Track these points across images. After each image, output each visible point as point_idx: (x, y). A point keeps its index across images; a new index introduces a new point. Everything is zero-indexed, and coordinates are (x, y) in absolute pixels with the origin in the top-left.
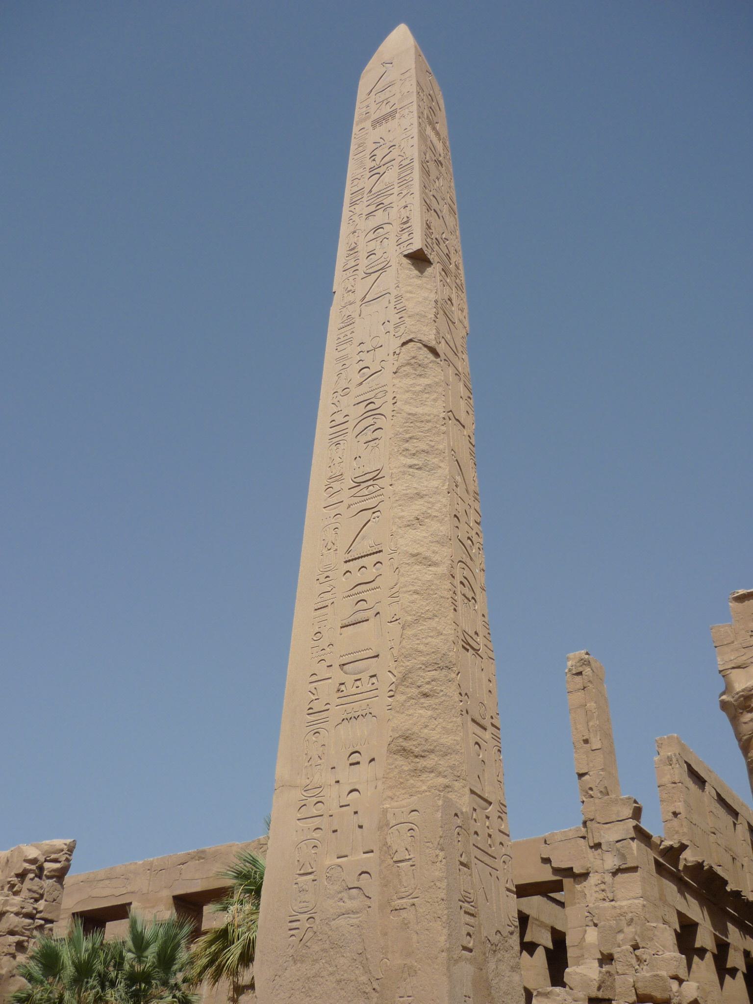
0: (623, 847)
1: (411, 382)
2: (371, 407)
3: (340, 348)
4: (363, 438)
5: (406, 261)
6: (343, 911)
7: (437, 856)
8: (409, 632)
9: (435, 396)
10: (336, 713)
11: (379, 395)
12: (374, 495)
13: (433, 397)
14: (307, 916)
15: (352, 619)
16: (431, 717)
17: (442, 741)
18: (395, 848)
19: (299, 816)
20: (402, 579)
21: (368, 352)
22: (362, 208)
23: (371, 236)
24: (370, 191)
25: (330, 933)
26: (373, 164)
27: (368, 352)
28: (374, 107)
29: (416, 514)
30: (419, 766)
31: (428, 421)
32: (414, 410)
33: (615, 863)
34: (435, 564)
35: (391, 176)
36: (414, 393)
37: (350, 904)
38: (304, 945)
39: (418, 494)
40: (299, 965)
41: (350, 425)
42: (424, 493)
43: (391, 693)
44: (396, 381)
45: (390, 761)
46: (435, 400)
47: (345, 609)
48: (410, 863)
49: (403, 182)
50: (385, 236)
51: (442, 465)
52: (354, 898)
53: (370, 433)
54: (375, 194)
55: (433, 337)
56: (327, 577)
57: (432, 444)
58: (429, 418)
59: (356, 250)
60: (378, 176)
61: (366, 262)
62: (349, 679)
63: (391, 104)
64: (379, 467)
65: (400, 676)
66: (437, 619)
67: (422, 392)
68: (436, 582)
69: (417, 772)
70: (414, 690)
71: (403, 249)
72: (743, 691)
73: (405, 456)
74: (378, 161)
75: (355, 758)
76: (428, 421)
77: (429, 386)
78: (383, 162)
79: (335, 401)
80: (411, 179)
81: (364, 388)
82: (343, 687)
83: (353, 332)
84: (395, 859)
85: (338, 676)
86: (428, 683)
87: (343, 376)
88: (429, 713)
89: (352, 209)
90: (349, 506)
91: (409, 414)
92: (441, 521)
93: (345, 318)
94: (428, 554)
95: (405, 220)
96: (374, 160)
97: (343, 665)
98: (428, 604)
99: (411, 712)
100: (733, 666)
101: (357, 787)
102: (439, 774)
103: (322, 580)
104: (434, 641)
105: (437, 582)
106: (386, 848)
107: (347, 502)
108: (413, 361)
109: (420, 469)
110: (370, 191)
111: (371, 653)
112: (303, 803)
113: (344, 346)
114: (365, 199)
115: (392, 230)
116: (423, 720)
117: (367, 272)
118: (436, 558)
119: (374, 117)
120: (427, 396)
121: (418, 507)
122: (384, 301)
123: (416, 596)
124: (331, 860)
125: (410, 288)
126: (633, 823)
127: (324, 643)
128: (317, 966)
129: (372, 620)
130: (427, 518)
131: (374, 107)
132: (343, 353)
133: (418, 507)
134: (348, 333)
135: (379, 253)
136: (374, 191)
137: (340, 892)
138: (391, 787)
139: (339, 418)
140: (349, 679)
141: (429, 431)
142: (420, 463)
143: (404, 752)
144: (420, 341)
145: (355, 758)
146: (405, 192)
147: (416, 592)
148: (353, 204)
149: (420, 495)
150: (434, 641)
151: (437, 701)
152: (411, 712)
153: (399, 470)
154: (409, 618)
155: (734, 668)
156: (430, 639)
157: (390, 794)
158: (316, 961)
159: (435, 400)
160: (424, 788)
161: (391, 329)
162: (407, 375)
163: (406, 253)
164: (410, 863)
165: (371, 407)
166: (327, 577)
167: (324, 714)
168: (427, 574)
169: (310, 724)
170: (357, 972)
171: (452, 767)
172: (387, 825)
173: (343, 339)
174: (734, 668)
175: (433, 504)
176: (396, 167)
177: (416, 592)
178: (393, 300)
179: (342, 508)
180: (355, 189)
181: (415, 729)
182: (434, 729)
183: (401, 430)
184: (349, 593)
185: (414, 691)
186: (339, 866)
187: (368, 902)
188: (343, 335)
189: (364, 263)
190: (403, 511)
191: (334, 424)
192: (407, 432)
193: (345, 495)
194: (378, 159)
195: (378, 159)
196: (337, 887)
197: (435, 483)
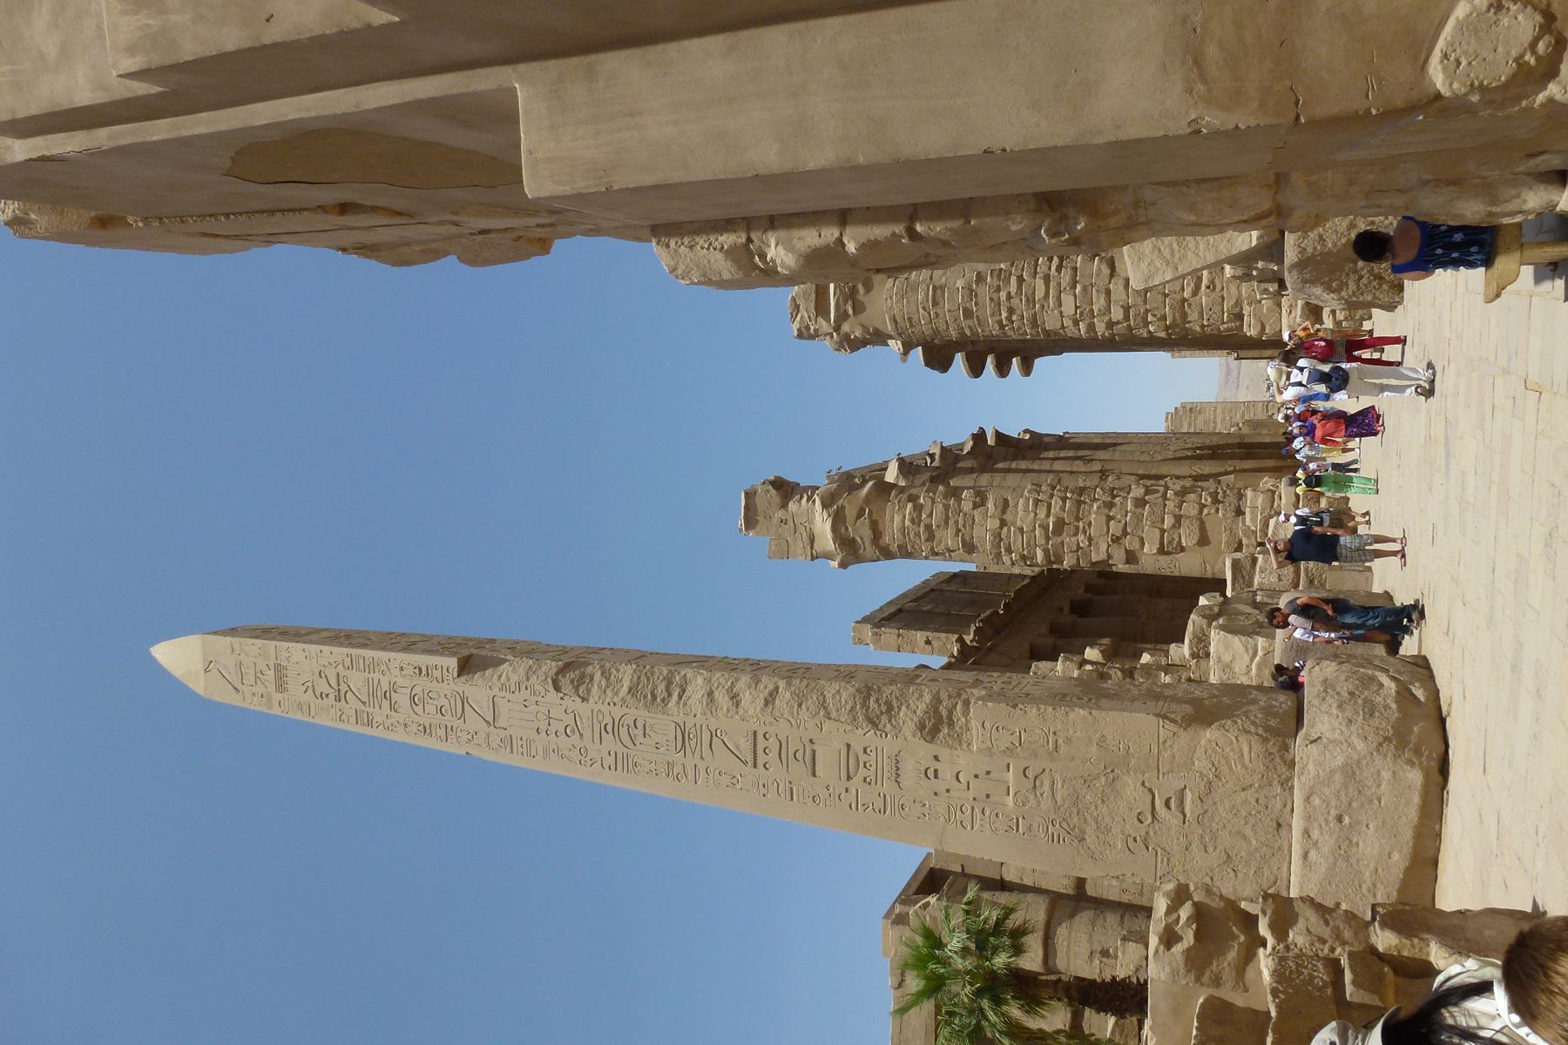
1: (596, 686)
2: (609, 728)
3: (533, 753)
4: (640, 738)
5: (463, 678)
6: (1050, 793)
7: (1021, 709)
8: (834, 715)
9: (613, 670)
10: (888, 787)
11: (600, 717)
12: (699, 733)
13: (615, 672)
15: (809, 763)
16: (908, 707)
17: (928, 701)
18: (1009, 745)
19: (969, 828)
20: (786, 715)
22: (379, 715)
23: (419, 709)
24: (364, 703)
25: (1066, 806)
26: (332, 697)
28: (259, 689)
29: (727, 698)
30: (945, 721)
31: (639, 678)
32: (625, 689)
34: (777, 689)
35: (356, 680)
36: (607, 687)
37: (1046, 788)
38: (1072, 830)
39: (709, 695)
40: (1086, 837)
41: (620, 749)
42: (708, 689)
43: (883, 735)
44: (591, 700)
45: (939, 742)
46: (618, 671)
47: (799, 770)
48: (1022, 732)
49: (372, 667)
50: (426, 692)
51: (683, 673)
52: (1042, 783)
53: (636, 731)
55: (554, 664)
56: (764, 787)
57: (661, 678)
58: (635, 678)
59: (428, 727)
60: (349, 693)
61: (448, 717)
62: (862, 772)
63: (265, 668)
64: (673, 725)
65: (870, 726)
66: (826, 693)
67: (608, 679)
68: (793, 689)
69: (951, 724)
70: (883, 718)
71: (450, 678)
72: (835, 543)
73: (669, 701)
74: (331, 691)
75: (931, 774)
76: (639, 678)
77: (603, 673)
78: (335, 687)
79: (589, 763)
80: (371, 659)
81: (587, 734)
82: (868, 780)
83: (521, 739)
84: (1017, 745)
85: (857, 780)
86: (879, 706)
87: (566, 752)
88: (904, 708)
89: (375, 725)
90: (702, 758)
91: (629, 692)
92: (737, 680)
93: (502, 745)
94: (767, 692)
95: (417, 671)
96: (327, 695)
98: (812, 698)
99: (901, 722)
100: (809, 547)
101: (954, 774)
102: (955, 707)
104: (844, 696)
105: (793, 689)
106: (1009, 751)
107: (697, 760)
108: (576, 683)
109: (684, 691)
110: (364, 703)
113: (533, 749)
114: (371, 710)
115: (422, 684)
116: (909, 713)
117: (459, 716)
118: (771, 687)
119: (272, 688)
120: (612, 677)
121: (721, 697)
122: (500, 702)
123: (803, 706)
124: (1010, 800)
125: (495, 677)
127: (823, 793)
128: (1089, 819)
129: (815, 747)
130: (732, 690)
131: (259, 689)
132: (540, 752)
133: (721, 697)
134: (520, 743)
135: (443, 701)
136: (365, 699)
137: (1036, 795)
138: (960, 744)
139: (610, 761)
141: (648, 680)
142: (678, 690)
143: (935, 730)
144: (557, 674)
145: (931, 774)
146: (384, 667)
147: (800, 705)
148: (370, 724)
149: (710, 694)
150: (844, 696)
151: (894, 701)
152: (901, 722)
153: (681, 707)
154: (822, 713)
155: (812, 548)
156: (843, 700)
157: (965, 745)
158: (1085, 820)
159: (618, 671)
160: (963, 719)
161: (534, 699)
162: (589, 691)
163: (456, 674)
164: (1022, 732)
165: (609, 728)
166: (764, 787)
167: (888, 797)
168: (785, 695)
170: (1097, 785)
171: (950, 697)
172: (990, 749)
173: (525, 750)
174: (812, 548)
175: (719, 684)
176: (348, 673)
177: (800, 705)
178: (503, 694)
179: (701, 766)
180: (353, 719)
181: (916, 719)
182: (918, 707)
183: (643, 701)
184: (785, 766)
185: (884, 718)
186: (1016, 794)
187: (1047, 771)
189: (448, 720)
190: (722, 708)
191: (613, 768)
192: (645, 697)
193: (690, 762)
194: (327, 690)
195: (327, 690)
196: (1032, 797)
197: (700, 680)
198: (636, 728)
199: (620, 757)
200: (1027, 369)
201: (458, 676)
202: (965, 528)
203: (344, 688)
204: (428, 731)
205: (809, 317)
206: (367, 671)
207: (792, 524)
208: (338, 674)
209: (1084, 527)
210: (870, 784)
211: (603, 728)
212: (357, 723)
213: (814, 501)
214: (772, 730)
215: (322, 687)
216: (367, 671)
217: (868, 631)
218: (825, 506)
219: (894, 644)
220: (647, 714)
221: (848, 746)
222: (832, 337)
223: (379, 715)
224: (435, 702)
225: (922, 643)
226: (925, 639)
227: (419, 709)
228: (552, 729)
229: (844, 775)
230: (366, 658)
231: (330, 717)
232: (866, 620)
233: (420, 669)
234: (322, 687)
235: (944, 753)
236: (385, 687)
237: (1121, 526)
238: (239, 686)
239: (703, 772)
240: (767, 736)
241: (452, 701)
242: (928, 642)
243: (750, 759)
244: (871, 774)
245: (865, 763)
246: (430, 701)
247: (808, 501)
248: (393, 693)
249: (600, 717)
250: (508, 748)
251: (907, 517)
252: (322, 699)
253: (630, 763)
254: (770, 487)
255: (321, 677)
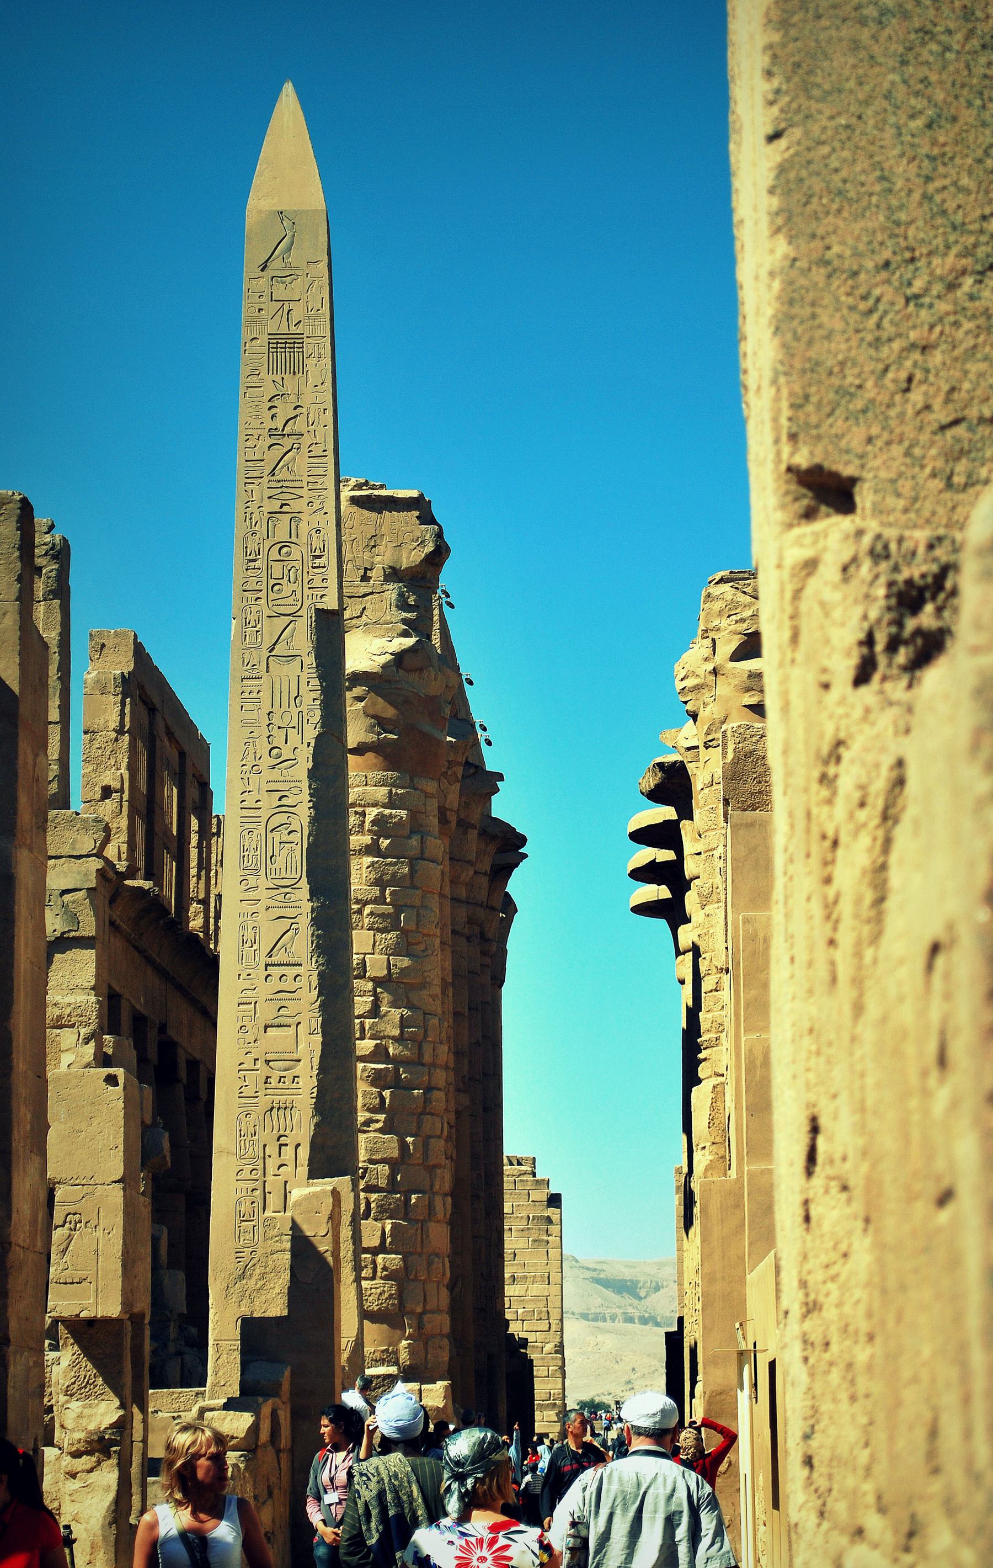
0: (73, 902)
14: (251, 1250)
15: (277, 1021)
19: (239, 1177)
21: (279, 728)
24: (272, 473)
27: (279, 728)
33: (57, 927)
50: (294, 564)
54: (279, 481)
59: (257, 564)
75: (283, 1140)
97: (270, 1061)
103: (243, 976)
110: (272, 473)
111: (295, 1056)
112: (241, 1168)
113: (250, 706)
126: (96, 864)
132: (249, 716)
134: (256, 689)
140: (276, 1075)
145: (283, 1140)
146: (316, 506)
148: (249, 480)
163: (319, 606)
169: (242, 1105)
176: (305, 450)
188: (249, 689)
193: (262, 894)
198: (289, 833)
199: (257, 813)
200: (644, 909)
201: (317, 610)
202: (372, 914)
203: (288, 443)
204: (252, 564)
205: (742, 620)
206: (311, 479)
207: (362, 590)
208: (303, 435)
209: (377, 1121)
210: (266, 1083)
211: (284, 793)
212: (246, 461)
213: (405, 634)
214: (303, 982)
215: (285, 411)
216: (311, 479)
217: (123, 664)
218: (400, 658)
219: (99, 722)
220: (305, 846)
221: (299, 1061)
222: (706, 660)
223: (260, 490)
224: (286, 579)
225: (109, 778)
226: (116, 785)
227: (274, 554)
228: (275, 732)
229: (269, 1057)
230: (324, 479)
231: (249, 420)
232: (140, 652)
233: (319, 557)
234: (285, 411)
235: (304, 1153)
236: (295, 505)
237: (383, 1183)
238: (269, 273)
239: (254, 908)
240: (298, 979)
241: (290, 601)
242: (107, 792)
243: (274, 959)
244: (273, 1081)
245: (285, 1077)
246: (286, 572)
247: (404, 621)
248: (289, 516)
249: (295, 791)
250: (247, 674)
251: (387, 812)
252: (270, 408)
253: (251, 825)
254: (430, 548)
255: (295, 408)
